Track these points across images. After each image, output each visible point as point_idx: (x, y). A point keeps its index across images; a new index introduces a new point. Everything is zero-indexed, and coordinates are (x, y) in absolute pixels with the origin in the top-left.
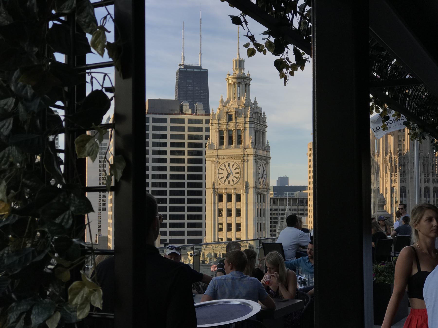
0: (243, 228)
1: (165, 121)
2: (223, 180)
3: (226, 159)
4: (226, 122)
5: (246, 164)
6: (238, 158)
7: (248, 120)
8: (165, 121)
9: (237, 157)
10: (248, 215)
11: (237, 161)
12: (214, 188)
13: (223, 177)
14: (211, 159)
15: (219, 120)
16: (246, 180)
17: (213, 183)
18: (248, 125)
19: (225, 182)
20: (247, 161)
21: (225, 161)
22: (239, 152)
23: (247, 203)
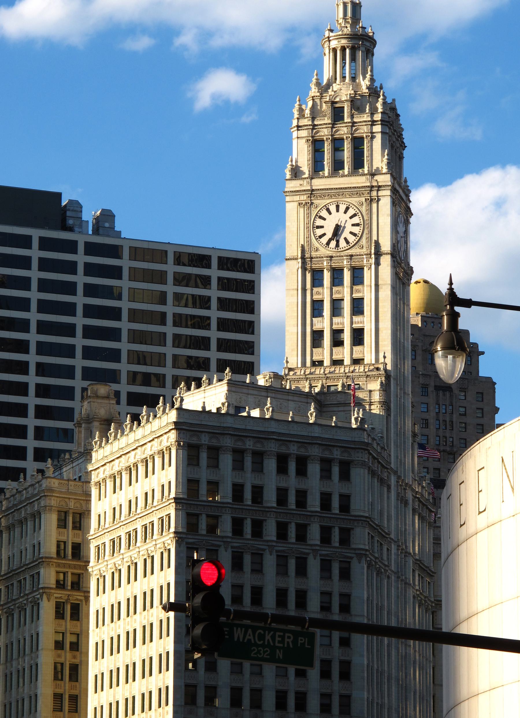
0: (369, 338)
1: (25, 242)
2: (324, 240)
3: (330, 196)
4: (330, 121)
5: (374, 205)
6: (359, 194)
7: (378, 117)
8: (25, 242)
9: (355, 191)
10: (380, 310)
11: (355, 200)
12: (303, 258)
13: (324, 234)
14: (297, 198)
15: (313, 119)
16: (375, 238)
17: (303, 247)
18: (377, 128)
19: (328, 243)
20: (379, 200)
21: (328, 201)
22: (360, 181)
23: (377, 285)
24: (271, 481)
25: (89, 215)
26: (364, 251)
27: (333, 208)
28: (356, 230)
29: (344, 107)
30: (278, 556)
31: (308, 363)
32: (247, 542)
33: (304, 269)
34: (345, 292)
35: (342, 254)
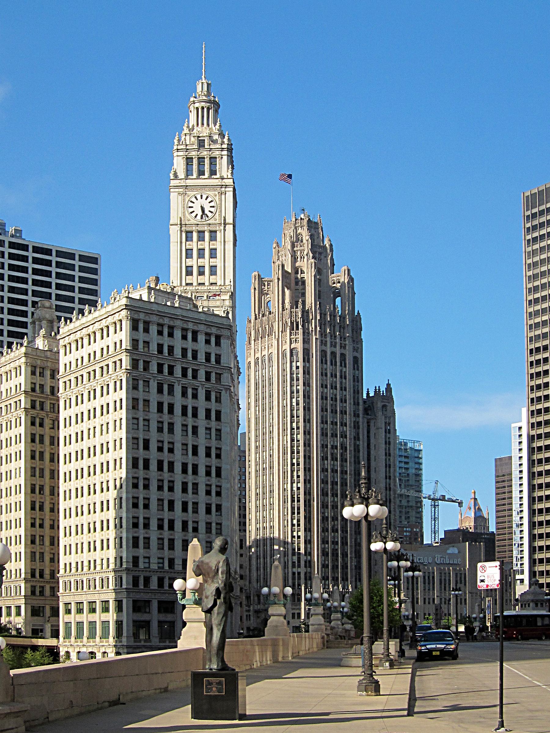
5: (223, 196)
11: (211, 193)
12: (181, 224)
16: (223, 215)
25: (11, 230)
27: (199, 197)
28: (212, 209)
31: (184, 284)
33: (181, 231)
35: (204, 223)
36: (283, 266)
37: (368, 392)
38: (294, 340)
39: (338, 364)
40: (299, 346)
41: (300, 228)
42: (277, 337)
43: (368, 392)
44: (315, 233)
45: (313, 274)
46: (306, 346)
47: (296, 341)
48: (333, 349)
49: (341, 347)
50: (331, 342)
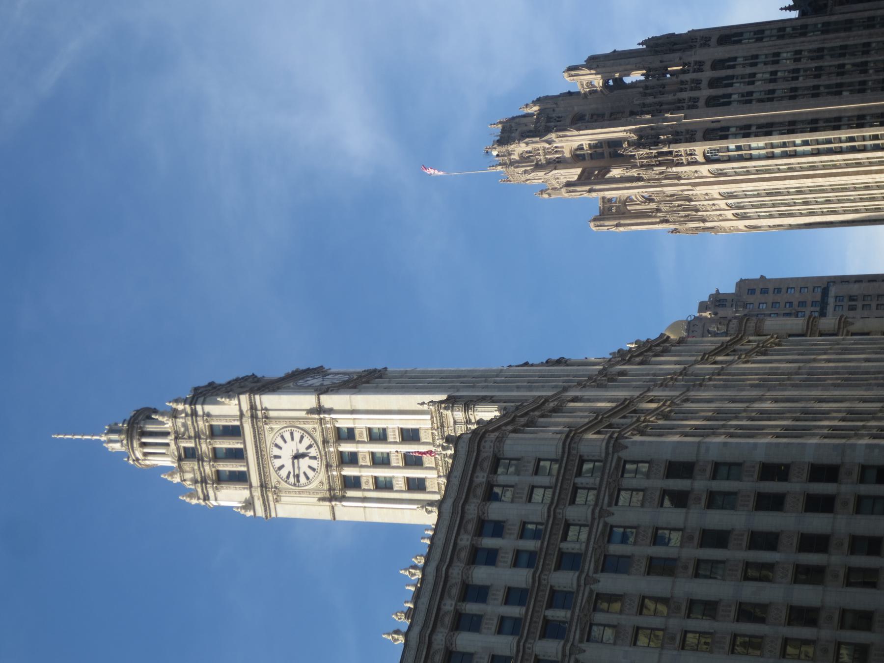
10: (377, 408)
14: (272, 504)
17: (320, 499)
18: (199, 408)
20: (266, 409)
21: (271, 468)
23: (353, 412)
24: (500, 576)
26: (317, 426)
27: (278, 463)
28: (297, 436)
29: (185, 448)
30: (602, 571)
32: (576, 617)
33: (343, 498)
34: (364, 449)
35: (323, 453)
36: (569, 184)
37: (786, 9)
38: (689, 158)
39: (730, 72)
40: (700, 149)
41: (512, 157)
42: (690, 187)
43: (786, 9)
44: (519, 130)
45: (576, 133)
46: (699, 135)
47: (691, 154)
48: (704, 84)
49: (700, 70)
50: (692, 89)
